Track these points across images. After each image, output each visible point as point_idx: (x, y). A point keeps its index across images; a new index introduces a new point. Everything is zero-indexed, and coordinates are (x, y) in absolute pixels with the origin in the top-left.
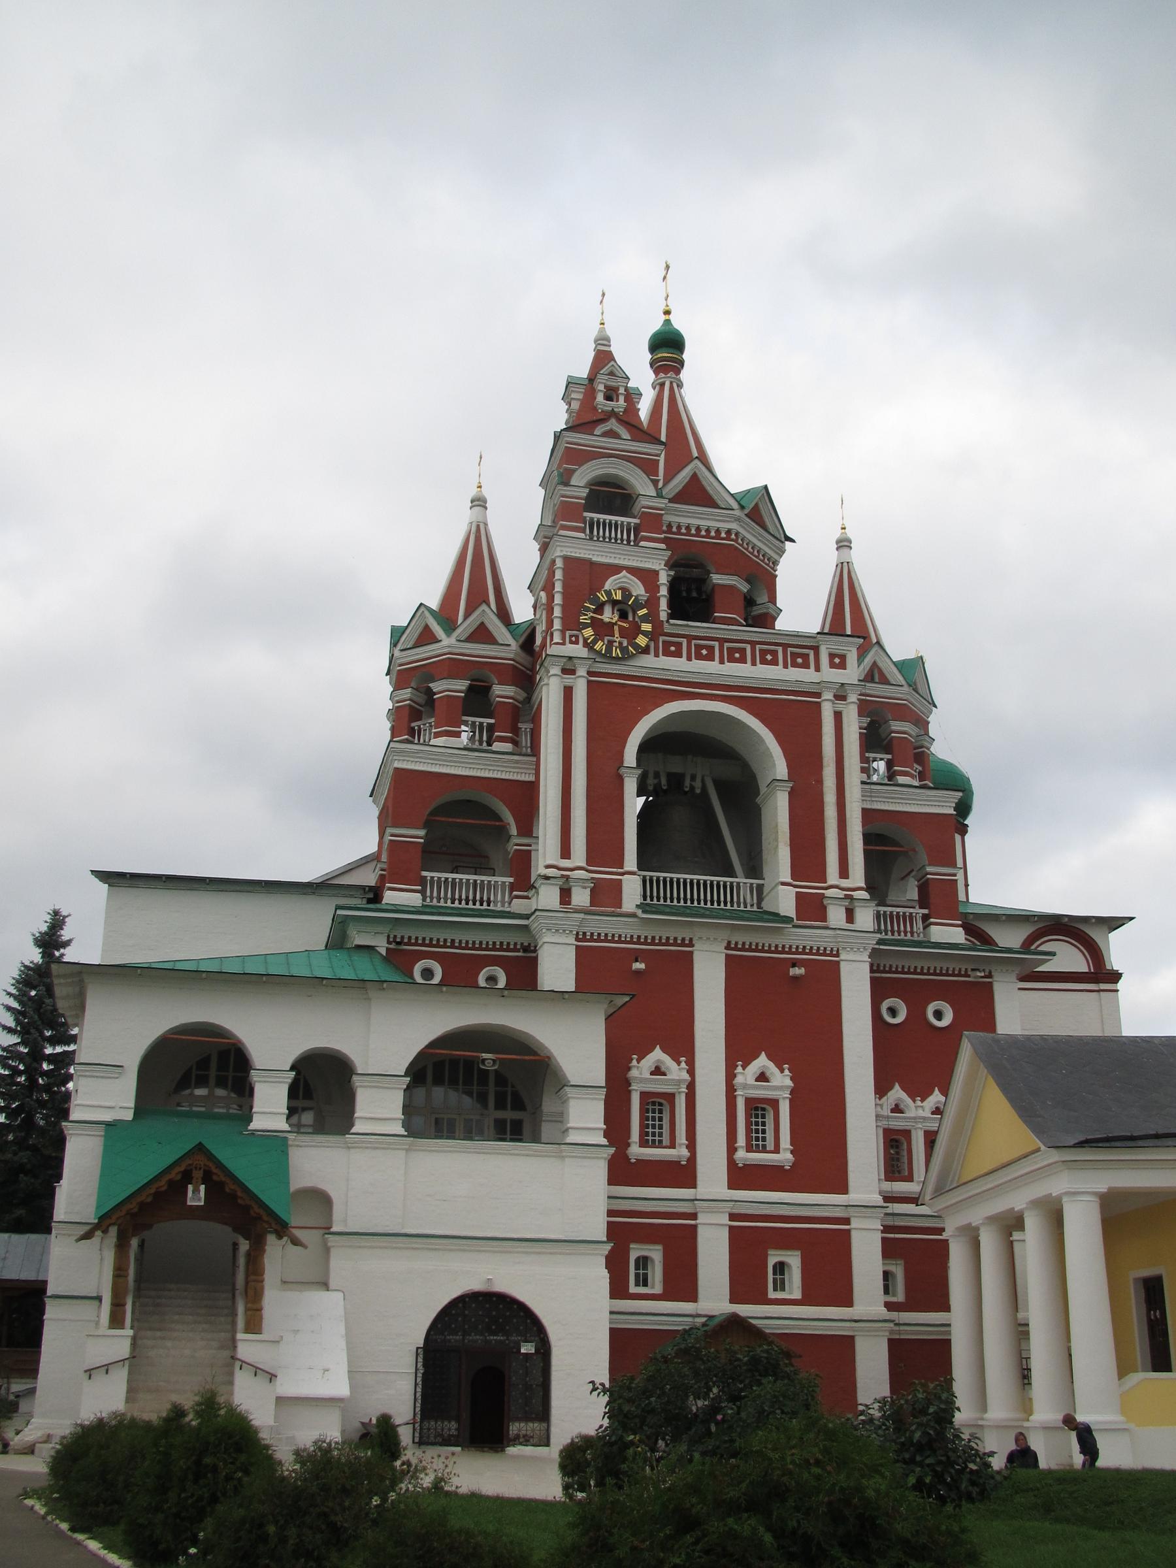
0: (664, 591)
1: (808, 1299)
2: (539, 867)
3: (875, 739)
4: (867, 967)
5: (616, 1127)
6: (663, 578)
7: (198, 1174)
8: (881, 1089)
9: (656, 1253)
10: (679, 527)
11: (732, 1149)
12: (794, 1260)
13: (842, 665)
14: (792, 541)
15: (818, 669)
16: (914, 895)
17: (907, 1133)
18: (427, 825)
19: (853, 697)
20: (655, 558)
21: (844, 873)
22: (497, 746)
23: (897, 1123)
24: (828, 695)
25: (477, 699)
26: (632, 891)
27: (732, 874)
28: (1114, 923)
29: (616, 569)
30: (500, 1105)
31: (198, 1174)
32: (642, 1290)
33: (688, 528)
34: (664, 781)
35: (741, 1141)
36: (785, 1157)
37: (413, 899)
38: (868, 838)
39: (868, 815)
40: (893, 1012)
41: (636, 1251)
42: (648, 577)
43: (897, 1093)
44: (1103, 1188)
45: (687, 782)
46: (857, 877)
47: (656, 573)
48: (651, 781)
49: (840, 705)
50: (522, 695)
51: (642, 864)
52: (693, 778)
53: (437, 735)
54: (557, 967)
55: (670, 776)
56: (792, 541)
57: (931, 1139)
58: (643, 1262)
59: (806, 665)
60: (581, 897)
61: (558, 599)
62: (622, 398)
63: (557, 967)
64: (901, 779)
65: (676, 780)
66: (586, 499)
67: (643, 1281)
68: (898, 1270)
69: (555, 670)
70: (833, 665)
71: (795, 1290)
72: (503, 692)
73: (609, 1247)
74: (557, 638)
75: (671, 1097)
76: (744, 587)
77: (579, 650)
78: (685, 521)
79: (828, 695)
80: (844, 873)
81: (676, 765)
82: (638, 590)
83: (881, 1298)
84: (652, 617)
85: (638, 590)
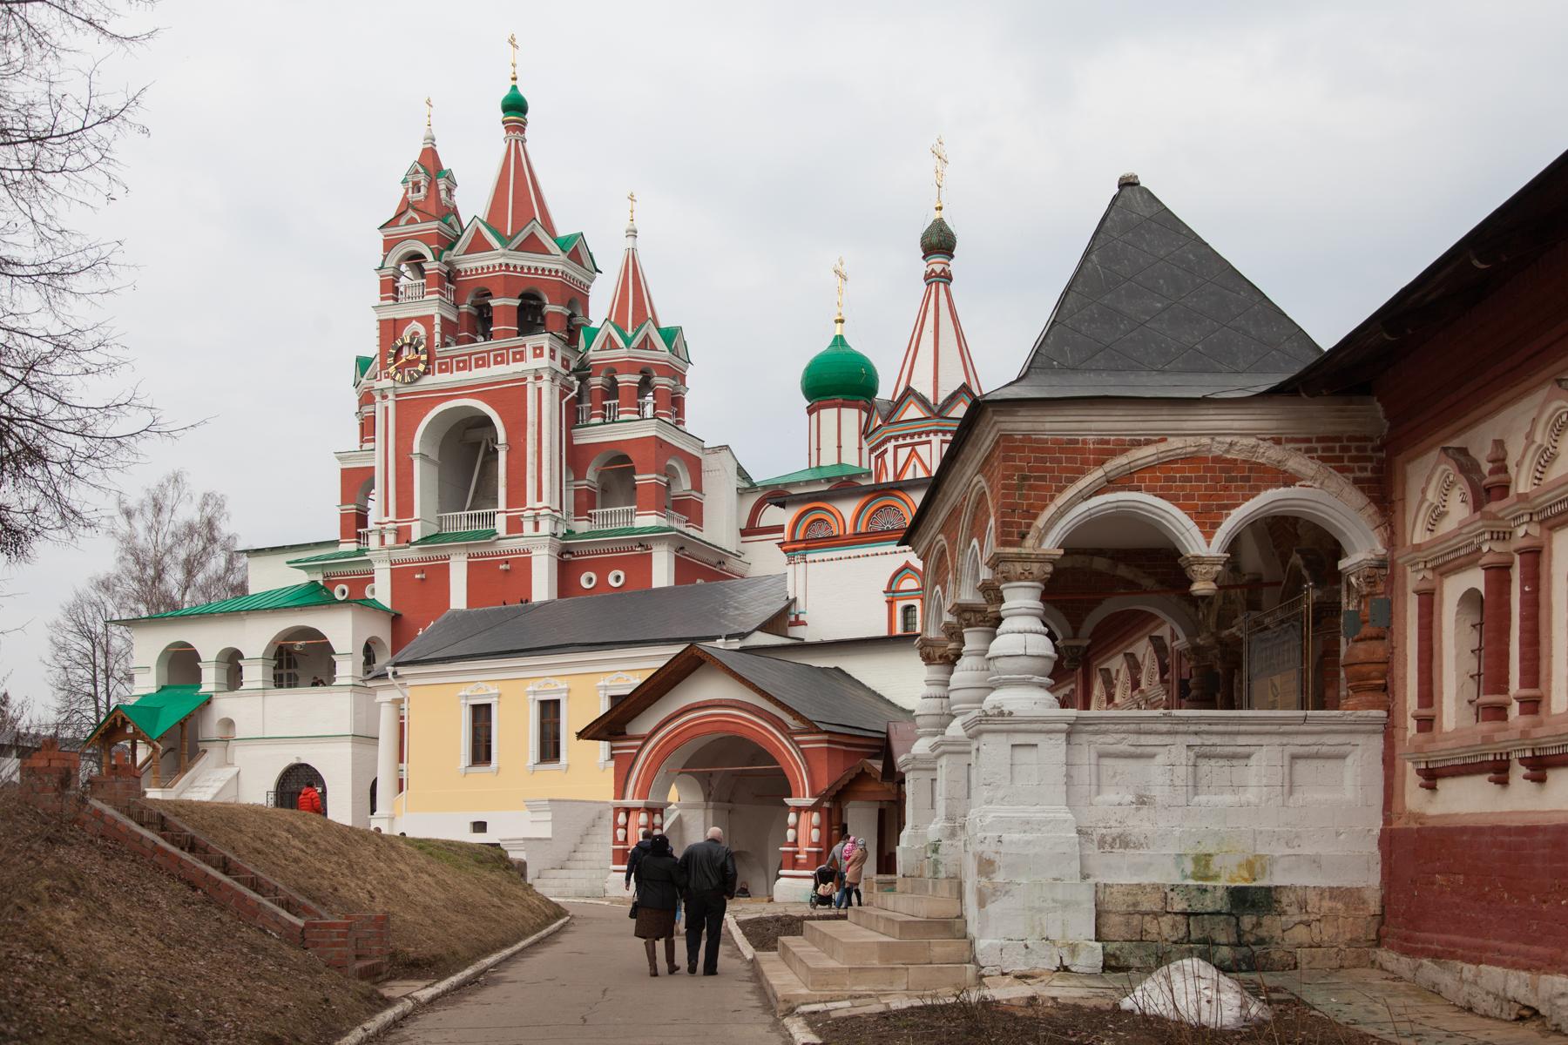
0: (437, 329)
6: (437, 320)
13: (541, 355)
24: (530, 379)
29: (409, 320)
42: (426, 321)
49: (539, 383)
59: (521, 360)
64: (622, 417)
70: (535, 356)
77: (387, 383)
79: (530, 379)
82: (422, 331)
84: (429, 351)
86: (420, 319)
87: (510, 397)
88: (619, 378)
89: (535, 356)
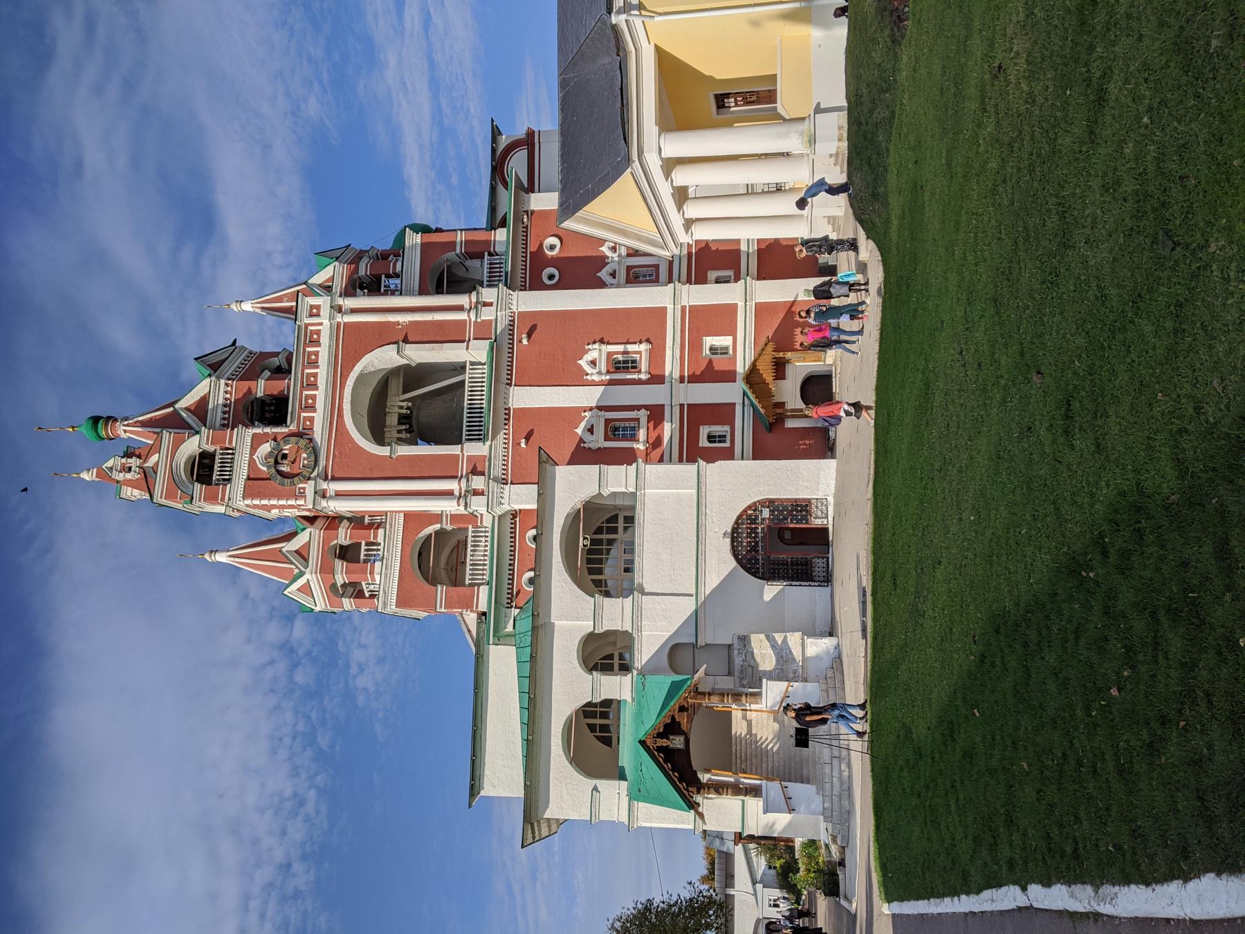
0: (267, 430)
1: (733, 333)
2: (461, 510)
3: (372, 286)
4: (521, 293)
5: (627, 457)
6: (259, 431)
7: (663, 742)
8: (602, 285)
9: (704, 431)
10: (224, 419)
11: (639, 382)
12: (709, 341)
13: (318, 307)
14: (235, 341)
15: (321, 324)
16: (476, 263)
17: (629, 268)
18: (433, 581)
19: (340, 301)
20: (244, 436)
21: (460, 308)
22: (380, 539)
23: (622, 275)
25: (347, 553)
26: (474, 449)
27: (463, 382)
28: (496, 133)
29: (252, 462)
30: (614, 530)
31: (663, 742)
32: (728, 439)
33: (224, 413)
34: (404, 427)
35: (635, 376)
36: (643, 347)
37: (484, 591)
38: (439, 291)
39: (423, 292)
40: (551, 277)
41: (703, 442)
42: (257, 442)
43: (604, 274)
44: (655, 129)
45: (404, 411)
46: (462, 300)
47: (254, 435)
48: (403, 435)
50: (345, 523)
51: (458, 441)
52: (401, 407)
53: (373, 579)
54: (523, 498)
55: (400, 423)
56: (235, 341)
57: (634, 253)
58: (711, 438)
59: (318, 333)
60: (478, 482)
61: (274, 502)
62: (130, 460)
63: (523, 498)
64: (398, 268)
65: (403, 419)
66: (202, 483)
67: (722, 438)
68: (712, 275)
69: (324, 503)
71: (725, 341)
72: (343, 536)
73: (702, 462)
74: (301, 502)
75: (607, 421)
76: (267, 374)
78: (219, 415)
80: (460, 308)
81: (392, 420)
82: (266, 448)
83: (732, 285)
85: (266, 448)
86: (253, 449)
87: (355, 341)
88: (362, 272)
89: (318, 315)
